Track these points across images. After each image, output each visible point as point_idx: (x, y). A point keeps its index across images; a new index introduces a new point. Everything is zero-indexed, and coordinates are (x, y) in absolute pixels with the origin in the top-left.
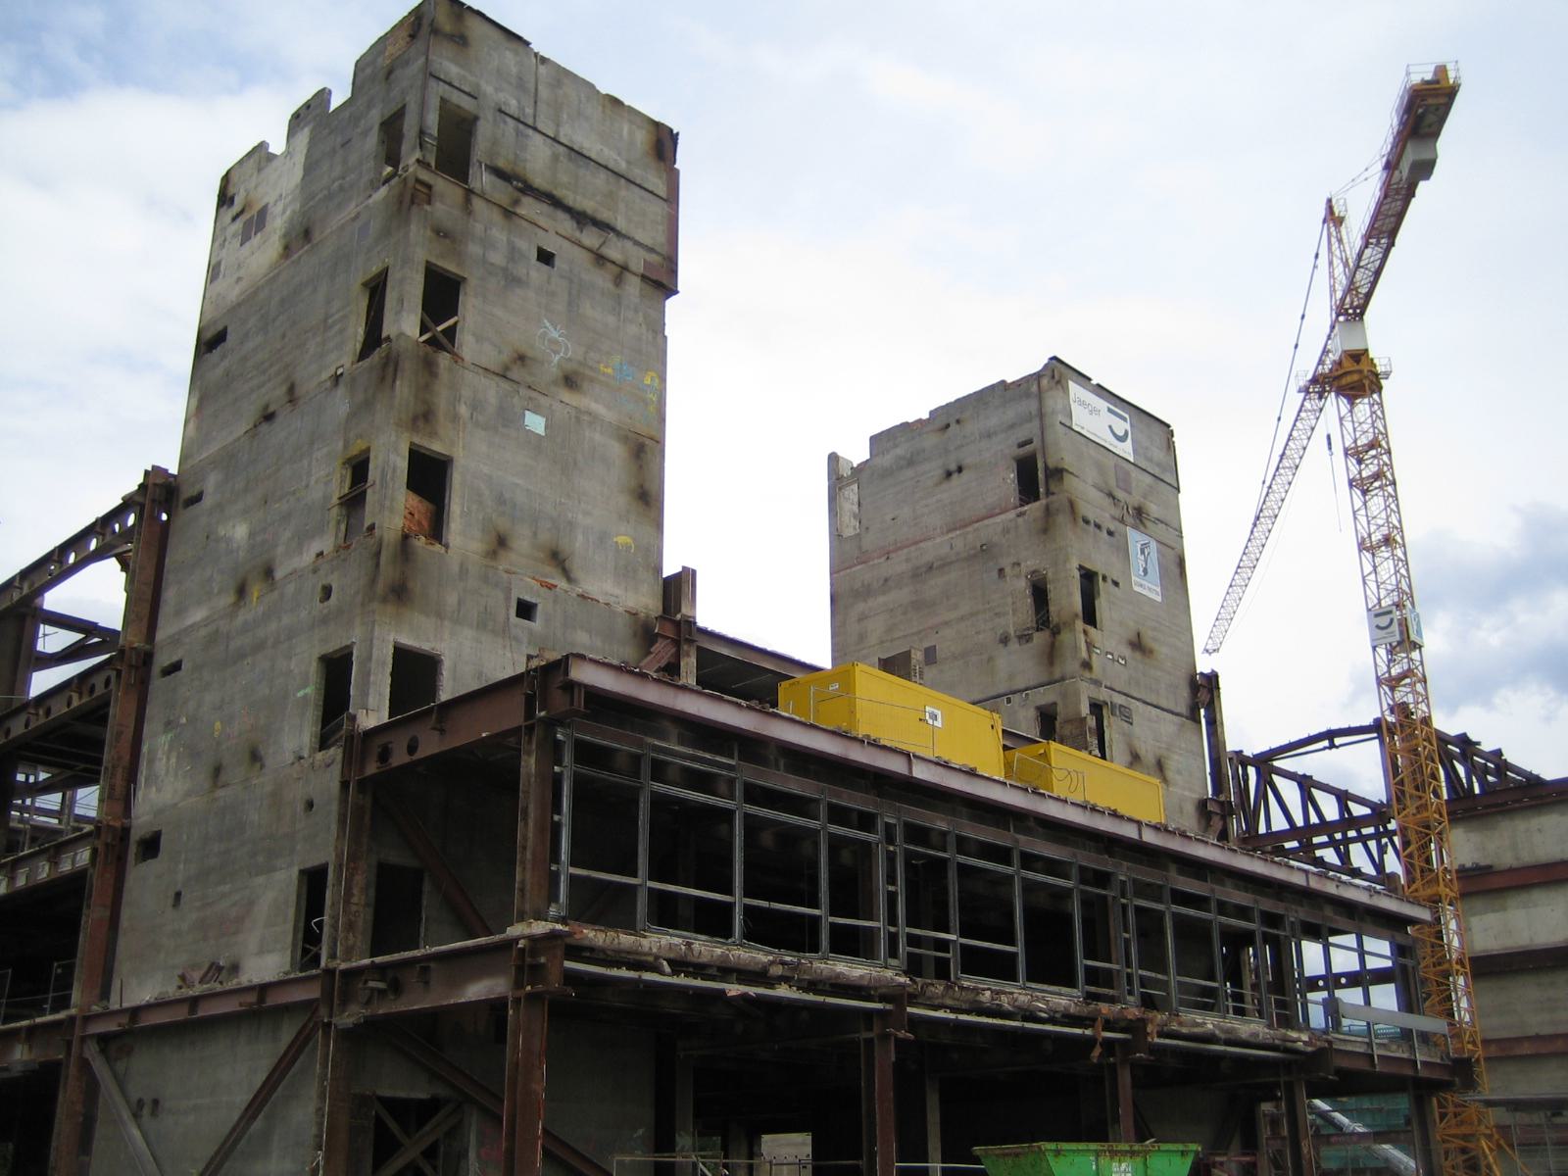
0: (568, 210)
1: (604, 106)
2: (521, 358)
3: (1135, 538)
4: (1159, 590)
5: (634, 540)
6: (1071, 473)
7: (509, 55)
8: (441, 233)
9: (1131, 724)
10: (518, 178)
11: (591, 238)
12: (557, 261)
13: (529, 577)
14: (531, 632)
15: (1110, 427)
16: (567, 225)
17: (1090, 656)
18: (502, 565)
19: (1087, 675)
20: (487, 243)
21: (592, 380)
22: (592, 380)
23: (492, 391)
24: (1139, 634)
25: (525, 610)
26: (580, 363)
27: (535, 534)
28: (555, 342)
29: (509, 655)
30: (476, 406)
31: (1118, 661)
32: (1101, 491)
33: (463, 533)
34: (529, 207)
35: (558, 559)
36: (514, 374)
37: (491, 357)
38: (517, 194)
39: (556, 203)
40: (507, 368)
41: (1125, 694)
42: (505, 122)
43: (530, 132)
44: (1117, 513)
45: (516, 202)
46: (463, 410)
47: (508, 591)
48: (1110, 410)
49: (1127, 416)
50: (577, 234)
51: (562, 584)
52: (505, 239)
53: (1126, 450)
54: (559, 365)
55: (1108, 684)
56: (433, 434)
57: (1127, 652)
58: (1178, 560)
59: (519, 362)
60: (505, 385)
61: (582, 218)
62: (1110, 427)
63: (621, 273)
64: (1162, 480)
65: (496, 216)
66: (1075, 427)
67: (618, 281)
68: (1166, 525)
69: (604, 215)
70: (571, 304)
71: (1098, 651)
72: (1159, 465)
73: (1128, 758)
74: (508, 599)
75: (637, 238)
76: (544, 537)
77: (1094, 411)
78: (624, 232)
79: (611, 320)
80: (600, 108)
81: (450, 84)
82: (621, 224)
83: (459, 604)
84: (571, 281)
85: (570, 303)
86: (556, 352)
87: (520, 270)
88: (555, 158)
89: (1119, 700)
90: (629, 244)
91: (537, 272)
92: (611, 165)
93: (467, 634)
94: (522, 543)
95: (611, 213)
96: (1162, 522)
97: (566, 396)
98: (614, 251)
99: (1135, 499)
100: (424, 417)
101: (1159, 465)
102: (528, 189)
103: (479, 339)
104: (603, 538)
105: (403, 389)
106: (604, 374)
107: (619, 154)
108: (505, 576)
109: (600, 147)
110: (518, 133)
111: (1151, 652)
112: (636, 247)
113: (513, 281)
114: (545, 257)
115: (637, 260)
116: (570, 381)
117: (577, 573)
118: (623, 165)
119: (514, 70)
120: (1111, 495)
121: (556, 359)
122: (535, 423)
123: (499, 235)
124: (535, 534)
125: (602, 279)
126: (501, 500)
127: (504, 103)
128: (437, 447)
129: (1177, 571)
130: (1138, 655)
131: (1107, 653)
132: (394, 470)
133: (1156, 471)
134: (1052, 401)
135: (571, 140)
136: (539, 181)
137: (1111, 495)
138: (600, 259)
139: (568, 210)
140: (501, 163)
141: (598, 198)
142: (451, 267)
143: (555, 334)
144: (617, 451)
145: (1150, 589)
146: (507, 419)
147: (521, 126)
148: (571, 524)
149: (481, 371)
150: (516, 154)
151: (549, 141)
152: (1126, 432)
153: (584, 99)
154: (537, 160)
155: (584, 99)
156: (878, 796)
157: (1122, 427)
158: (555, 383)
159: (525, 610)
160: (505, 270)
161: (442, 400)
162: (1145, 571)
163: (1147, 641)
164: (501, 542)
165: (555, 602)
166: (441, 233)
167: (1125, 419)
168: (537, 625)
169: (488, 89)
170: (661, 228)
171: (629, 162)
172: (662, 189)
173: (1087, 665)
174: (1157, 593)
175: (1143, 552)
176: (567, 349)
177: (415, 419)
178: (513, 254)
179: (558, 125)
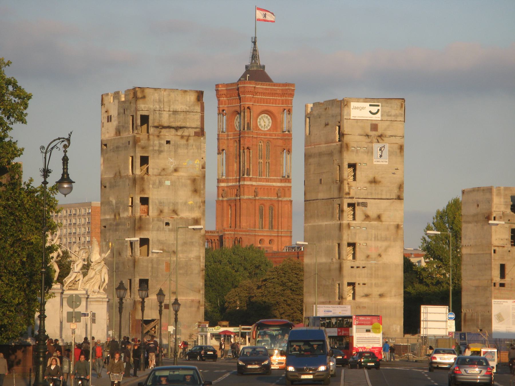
0: (173, 128)
1: (182, 95)
2: (164, 169)
3: (376, 147)
4: (387, 160)
5: (193, 202)
6: (349, 134)
7: (156, 94)
8: (143, 148)
9: (367, 207)
10: (160, 126)
11: (180, 133)
12: (171, 142)
13: (168, 217)
14: (169, 229)
15: (370, 112)
16: (173, 131)
17: (349, 191)
18: (161, 216)
19: (348, 196)
20: (153, 146)
21: (181, 168)
22: (181, 168)
23: (157, 179)
24: (374, 178)
25: (167, 224)
26: (178, 165)
27: (169, 208)
28: (172, 162)
29: (164, 234)
30: (154, 184)
31: (363, 189)
32: (361, 135)
33: (153, 212)
34: (164, 132)
35: (175, 212)
36: (162, 174)
37: (156, 172)
38: (160, 130)
39: (169, 127)
40: (160, 173)
41: (364, 198)
42: (156, 113)
43: (163, 112)
44: (369, 140)
45: (160, 132)
46: (151, 186)
47: (163, 222)
48: (370, 105)
49: (380, 104)
50: (176, 133)
51: (175, 216)
52: (158, 142)
53: (378, 116)
54: (173, 168)
55: (357, 197)
56: (145, 194)
57: (368, 185)
58: (399, 147)
59: (163, 171)
60: (160, 177)
61: (177, 128)
62: (370, 112)
63: (188, 138)
64: (396, 121)
65: (156, 138)
66: (352, 118)
67: (187, 140)
68: (395, 136)
69: (183, 125)
70: (175, 151)
71: (354, 188)
72: (394, 116)
73: (363, 217)
74: (163, 223)
75: (192, 127)
76: (171, 208)
77: (363, 108)
78: (189, 127)
79: (186, 151)
80: (181, 96)
81: (142, 110)
82: (188, 125)
83: (153, 227)
84: (175, 146)
85: (175, 151)
86: (172, 165)
87: (162, 149)
88: (170, 116)
89: (360, 201)
90: (190, 129)
91: (166, 147)
92: (184, 110)
93: (155, 232)
94: (166, 210)
95: (185, 123)
96: (392, 136)
97: (176, 174)
98: (186, 133)
99: (380, 132)
100: (143, 190)
101: (394, 116)
102: (164, 127)
103: (153, 169)
104: (185, 203)
105: (137, 187)
106: (184, 165)
107: (187, 106)
108: (162, 218)
109: (181, 106)
110: (160, 114)
111: (380, 182)
112: (192, 129)
113: (160, 152)
114: (168, 142)
115: (192, 132)
116: (176, 170)
117: (179, 213)
118: (188, 108)
119: (157, 98)
120: (367, 136)
121: (172, 166)
122: (168, 183)
123: (157, 142)
124: (169, 208)
125: (183, 142)
126: (160, 203)
127: (156, 108)
128: (146, 196)
129: (398, 151)
130: (373, 185)
131: (358, 188)
132: (137, 204)
133: (393, 118)
134: (345, 111)
135: (173, 109)
136: (166, 124)
137: (367, 136)
138: (182, 137)
139: (173, 128)
140: (156, 124)
141: (181, 121)
142: (145, 155)
143: (172, 160)
144: (189, 182)
145: (382, 161)
146: (161, 183)
147: (160, 112)
148: (177, 203)
149: (154, 176)
150: (159, 120)
151: (167, 112)
152: (378, 110)
153: (176, 95)
154: (165, 120)
155: (176, 95)
156: (260, 247)
157: (374, 109)
158: (172, 172)
159: (167, 224)
160: (158, 150)
161: (146, 187)
162: (381, 156)
163: (378, 178)
164: (161, 212)
165: (174, 221)
166: (143, 148)
167: (378, 106)
168: (170, 227)
169: (151, 106)
170: (199, 121)
171: (189, 107)
172: (198, 109)
173: (348, 194)
174: (386, 162)
175: (380, 150)
176: (175, 163)
177: (141, 192)
178: (160, 145)
179: (170, 107)
